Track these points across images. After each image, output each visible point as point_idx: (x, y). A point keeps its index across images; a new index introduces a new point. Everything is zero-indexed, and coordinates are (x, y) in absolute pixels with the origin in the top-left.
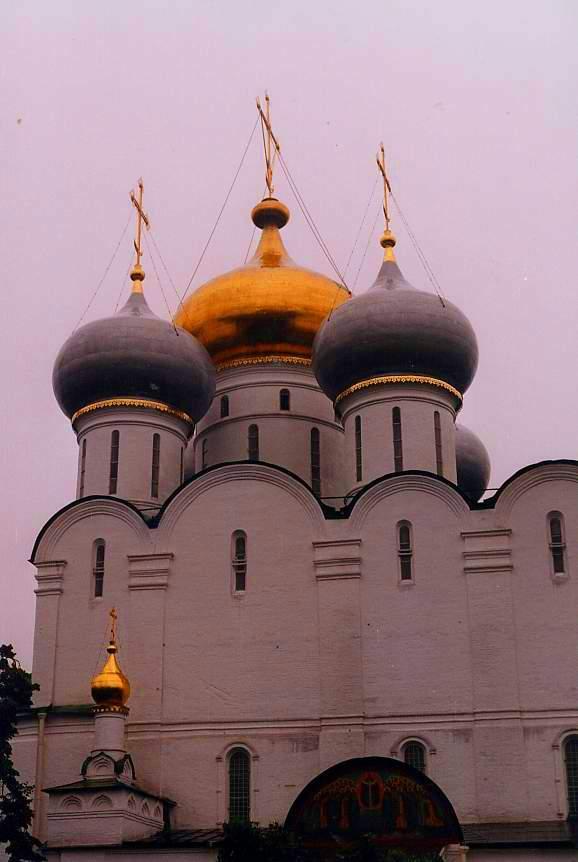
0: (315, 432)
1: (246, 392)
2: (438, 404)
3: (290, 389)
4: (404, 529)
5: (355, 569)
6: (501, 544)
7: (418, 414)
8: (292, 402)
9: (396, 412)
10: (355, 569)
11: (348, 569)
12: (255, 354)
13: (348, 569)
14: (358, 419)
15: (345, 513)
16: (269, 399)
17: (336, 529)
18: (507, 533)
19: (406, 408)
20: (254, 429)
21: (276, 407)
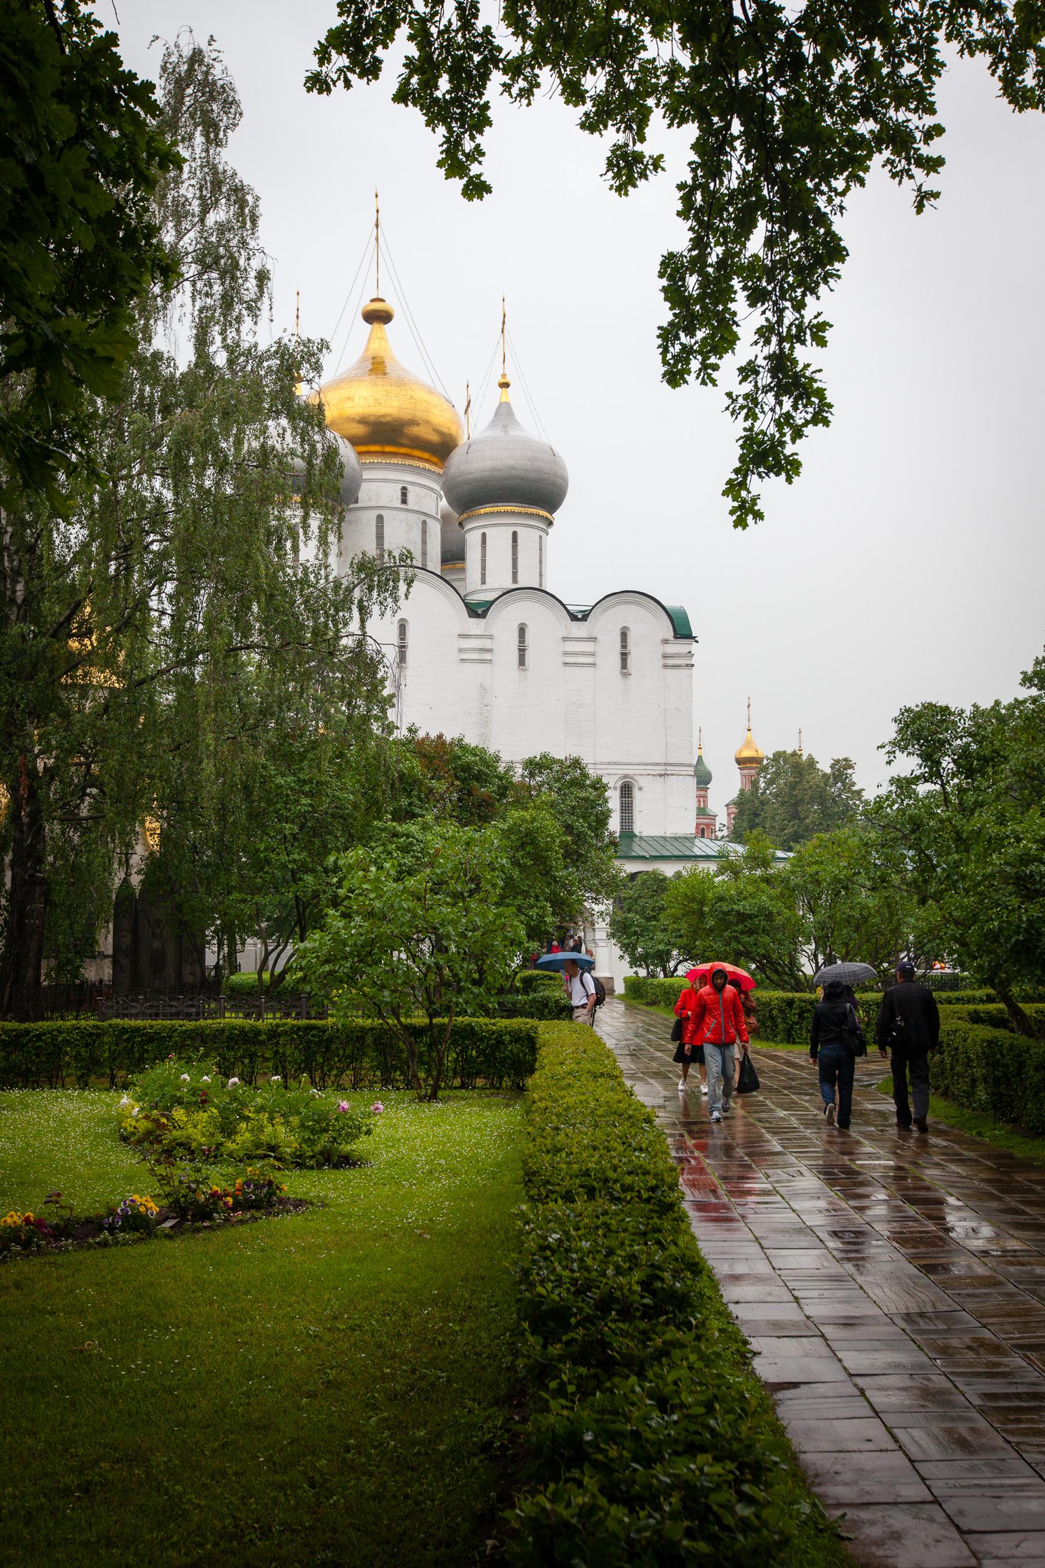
0: (424, 522)
1: (374, 486)
2: (542, 530)
3: (409, 487)
4: (522, 630)
5: (487, 656)
6: (588, 647)
7: (528, 536)
8: (410, 497)
9: (515, 534)
10: (487, 656)
11: (485, 656)
12: (383, 453)
13: (485, 656)
14: (484, 535)
15: (483, 615)
16: (390, 494)
17: (476, 626)
18: (593, 639)
19: (522, 532)
20: (380, 518)
21: (398, 503)
